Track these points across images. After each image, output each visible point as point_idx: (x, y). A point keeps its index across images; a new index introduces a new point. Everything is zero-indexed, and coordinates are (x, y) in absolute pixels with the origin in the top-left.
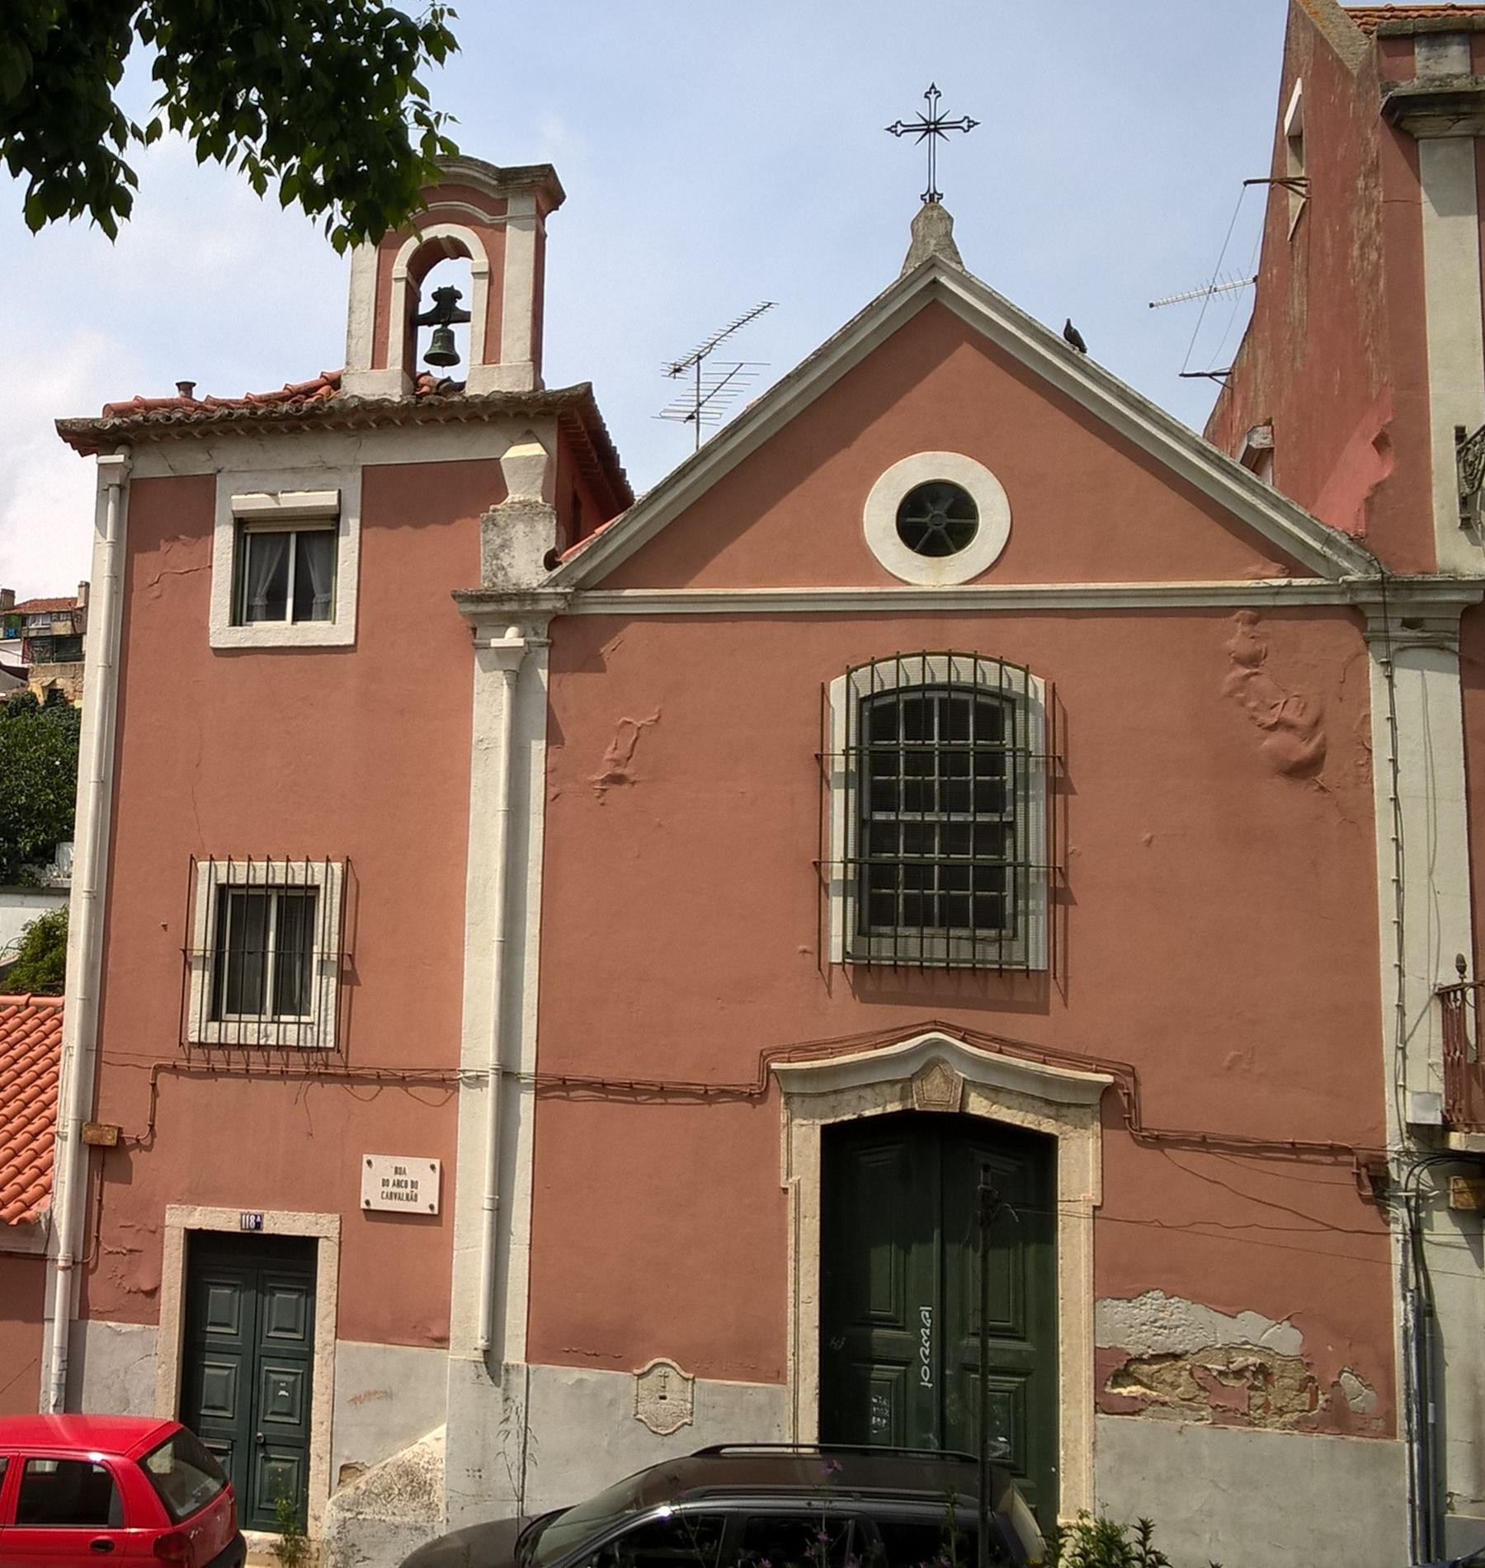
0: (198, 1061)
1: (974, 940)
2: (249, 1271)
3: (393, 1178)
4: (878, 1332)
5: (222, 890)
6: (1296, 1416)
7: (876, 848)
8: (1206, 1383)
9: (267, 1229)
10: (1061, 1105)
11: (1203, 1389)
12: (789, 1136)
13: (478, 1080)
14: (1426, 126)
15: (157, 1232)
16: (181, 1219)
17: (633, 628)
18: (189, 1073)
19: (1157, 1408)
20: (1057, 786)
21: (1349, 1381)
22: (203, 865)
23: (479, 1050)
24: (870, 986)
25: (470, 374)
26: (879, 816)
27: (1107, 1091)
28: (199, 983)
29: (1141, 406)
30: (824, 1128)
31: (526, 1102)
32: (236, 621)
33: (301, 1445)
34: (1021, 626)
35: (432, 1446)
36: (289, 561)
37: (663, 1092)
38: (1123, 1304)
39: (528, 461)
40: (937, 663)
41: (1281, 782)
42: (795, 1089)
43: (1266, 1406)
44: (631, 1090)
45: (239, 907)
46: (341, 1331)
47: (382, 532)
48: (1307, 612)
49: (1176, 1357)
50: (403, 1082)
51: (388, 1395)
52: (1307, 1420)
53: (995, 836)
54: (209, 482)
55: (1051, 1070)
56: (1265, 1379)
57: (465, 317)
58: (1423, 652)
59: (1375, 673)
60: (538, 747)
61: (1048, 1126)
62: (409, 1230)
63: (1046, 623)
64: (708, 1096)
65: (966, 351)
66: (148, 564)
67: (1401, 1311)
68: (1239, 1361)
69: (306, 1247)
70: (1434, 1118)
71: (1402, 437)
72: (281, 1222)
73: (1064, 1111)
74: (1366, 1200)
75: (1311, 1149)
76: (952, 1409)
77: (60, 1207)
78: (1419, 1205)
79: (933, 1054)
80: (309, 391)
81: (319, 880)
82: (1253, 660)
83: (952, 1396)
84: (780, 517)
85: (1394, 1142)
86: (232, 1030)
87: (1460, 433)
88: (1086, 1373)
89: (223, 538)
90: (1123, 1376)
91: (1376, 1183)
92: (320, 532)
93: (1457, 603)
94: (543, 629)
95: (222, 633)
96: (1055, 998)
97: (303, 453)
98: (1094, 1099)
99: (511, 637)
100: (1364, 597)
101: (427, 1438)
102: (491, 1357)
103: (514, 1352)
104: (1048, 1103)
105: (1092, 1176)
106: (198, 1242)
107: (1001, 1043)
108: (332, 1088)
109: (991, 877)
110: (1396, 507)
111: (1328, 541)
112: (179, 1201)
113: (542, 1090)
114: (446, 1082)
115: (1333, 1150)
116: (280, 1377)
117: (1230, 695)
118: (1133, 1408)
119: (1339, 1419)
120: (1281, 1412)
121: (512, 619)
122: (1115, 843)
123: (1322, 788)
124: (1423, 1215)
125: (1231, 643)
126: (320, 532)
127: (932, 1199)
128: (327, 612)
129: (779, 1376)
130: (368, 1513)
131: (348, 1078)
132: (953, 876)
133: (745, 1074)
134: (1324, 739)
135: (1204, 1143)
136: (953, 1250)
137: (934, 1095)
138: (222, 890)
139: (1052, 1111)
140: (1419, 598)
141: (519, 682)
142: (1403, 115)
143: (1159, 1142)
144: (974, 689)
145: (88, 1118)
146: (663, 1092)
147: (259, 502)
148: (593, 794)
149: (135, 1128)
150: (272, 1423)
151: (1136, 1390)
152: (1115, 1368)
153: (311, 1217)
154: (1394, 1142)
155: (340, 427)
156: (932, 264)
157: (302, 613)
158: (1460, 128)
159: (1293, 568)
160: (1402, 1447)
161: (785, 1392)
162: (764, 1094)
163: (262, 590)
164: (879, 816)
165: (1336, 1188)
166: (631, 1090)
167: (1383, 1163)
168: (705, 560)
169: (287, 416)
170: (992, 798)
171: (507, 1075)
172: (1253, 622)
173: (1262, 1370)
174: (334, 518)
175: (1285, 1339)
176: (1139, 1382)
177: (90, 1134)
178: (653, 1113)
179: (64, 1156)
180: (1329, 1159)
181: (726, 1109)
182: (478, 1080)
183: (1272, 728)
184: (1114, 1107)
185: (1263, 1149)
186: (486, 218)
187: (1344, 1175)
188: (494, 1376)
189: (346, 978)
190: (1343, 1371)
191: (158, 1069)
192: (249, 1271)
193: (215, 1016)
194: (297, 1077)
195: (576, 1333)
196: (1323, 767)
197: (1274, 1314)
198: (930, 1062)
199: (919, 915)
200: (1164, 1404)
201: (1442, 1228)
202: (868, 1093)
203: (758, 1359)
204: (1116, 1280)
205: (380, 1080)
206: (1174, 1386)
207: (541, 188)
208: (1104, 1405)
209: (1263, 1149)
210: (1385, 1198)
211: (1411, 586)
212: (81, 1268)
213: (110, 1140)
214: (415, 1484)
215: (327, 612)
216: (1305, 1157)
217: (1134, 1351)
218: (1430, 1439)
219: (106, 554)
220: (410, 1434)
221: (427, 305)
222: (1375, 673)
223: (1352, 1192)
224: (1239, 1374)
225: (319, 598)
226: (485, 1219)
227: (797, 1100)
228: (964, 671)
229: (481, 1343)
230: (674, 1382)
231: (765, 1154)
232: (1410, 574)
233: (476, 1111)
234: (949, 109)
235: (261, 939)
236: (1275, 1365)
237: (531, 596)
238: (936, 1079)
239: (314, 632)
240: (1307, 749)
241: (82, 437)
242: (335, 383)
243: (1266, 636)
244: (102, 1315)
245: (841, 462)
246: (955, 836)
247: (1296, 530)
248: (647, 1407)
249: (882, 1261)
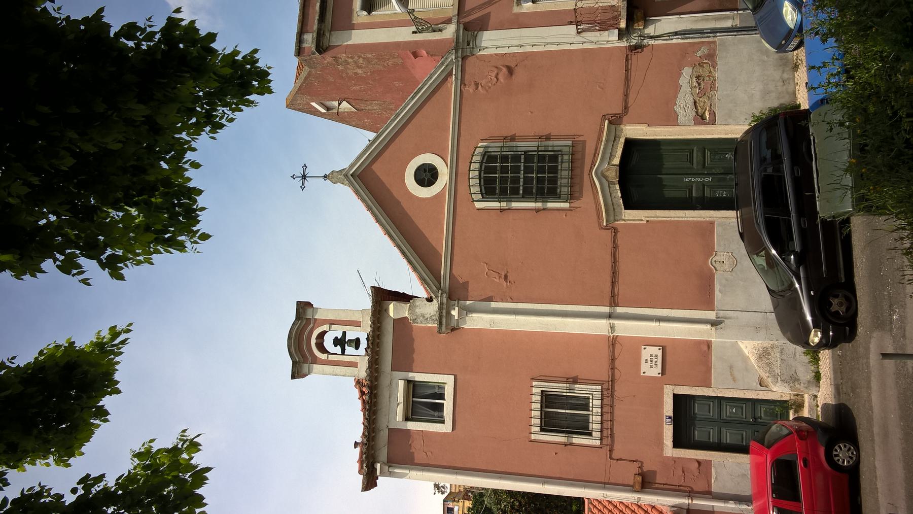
0: (607, 441)
1: (562, 162)
2: (688, 422)
3: (649, 364)
4: (694, 195)
5: (542, 430)
7: (532, 193)
8: (703, 93)
9: (671, 414)
13: (612, 327)
14: (325, 43)
15: (675, 460)
16: (669, 450)
17: (454, 272)
18: (612, 445)
20: (513, 138)
21: (699, 54)
22: (533, 437)
23: (600, 327)
24: (577, 195)
25: (362, 334)
26: (521, 192)
27: (610, 123)
28: (577, 440)
31: (619, 310)
32: (443, 422)
33: (754, 402)
34: (461, 150)
35: (748, 347)
36: (425, 403)
37: (614, 262)
39: (394, 308)
40: (472, 174)
41: (514, 77)
42: (612, 218)
43: (709, 76)
44: (614, 273)
45: (549, 424)
46: (708, 386)
47: (414, 364)
48: (463, 71)
49: (695, 102)
50: (613, 360)
51: (731, 367)
53: (528, 157)
54: (391, 431)
57: (344, 333)
59: (482, 53)
60: (494, 305)
61: (622, 140)
62: (668, 358)
63: (461, 143)
64: (615, 247)
65: (375, 167)
66: (419, 457)
67: (676, 40)
68: (695, 84)
69: (676, 397)
70: (616, 31)
71: (414, 50)
72: (668, 408)
74: (642, 51)
75: (627, 66)
76: (718, 171)
77: (665, 501)
78: (643, 37)
79: (599, 172)
80: (362, 393)
81: (539, 390)
82: (477, 85)
84: (421, 223)
85: (624, 44)
86: (595, 426)
87: (414, 32)
88: (703, 128)
89: (412, 426)
90: (702, 117)
92: (413, 387)
94: (453, 302)
95: (446, 428)
96: (581, 138)
97: (384, 393)
98: (613, 127)
99: (455, 313)
100: (460, 54)
101: (746, 351)
102: (714, 323)
103: (711, 315)
105: (638, 127)
106: (677, 444)
108: (617, 388)
109: (541, 158)
110: (435, 50)
111: (442, 64)
112: (662, 450)
113: (614, 301)
114: (613, 342)
115: (627, 60)
116: (729, 411)
118: (713, 114)
119: (711, 56)
120: (710, 72)
121: (448, 313)
125: (471, 91)
126: (413, 387)
128: (441, 386)
129: (712, 223)
130: (778, 371)
131: (613, 380)
132: (541, 170)
133: (608, 234)
135: (626, 95)
137: (613, 174)
138: (542, 430)
141: (470, 310)
142: (321, 48)
143: (626, 108)
144: (481, 163)
145: (631, 488)
146: (614, 262)
147: (400, 410)
148: (510, 287)
149: (634, 468)
150: (746, 414)
153: (665, 396)
154: (624, 44)
155: (377, 379)
156: (346, 176)
157: (442, 397)
158: (327, 35)
159: (450, 74)
160: (719, 38)
161: (717, 221)
162: (615, 228)
163: (432, 413)
164: (521, 192)
165: (638, 60)
166: (614, 273)
167: (630, 46)
169: (370, 407)
170: (516, 158)
171: (610, 316)
172: (465, 85)
173: (698, 77)
174: (408, 382)
175: (687, 72)
177: (638, 487)
178: (622, 266)
181: (619, 241)
182: (612, 327)
184: (616, 121)
185: (627, 79)
186: (311, 325)
187: (634, 57)
188: (721, 323)
189: (575, 381)
191: (611, 458)
192: (688, 422)
193: (590, 434)
194: (613, 401)
195: (702, 292)
196: (509, 66)
197: (679, 75)
198: (602, 176)
199: (554, 181)
201: (650, 30)
202: (613, 195)
203: (708, 229)
204: (671, 119)
205: (613, 369)
206: (705, 102)
207: (303, 307)
208: (713, 122)
209: (627, 79)
211: (457, 42)
212: (691, 493)
213: (639, 479)
214: (764, 354)
215: (441, 386)
218: (714, 31)
219: (414, 473)
220: (745, 359)
221: (338, 349)
223: (639, 55)
224: (699, 84)
225: (437, 390)
226: (664, 325)
229: (709, 326)
230: (717, 258)
231: (634, 227)
232: (454, 44)
234: (299, 172)
235: (562, 415)
237: (441, 304)
238: (608, 174)
239: (449, 392)
240: (505, 70)
241: (370, 483)
242: (359, 383)
244: (710, 485)
245: (404, 204)
246: (528, 170)
248: (727, 268)
249: (669, 193)
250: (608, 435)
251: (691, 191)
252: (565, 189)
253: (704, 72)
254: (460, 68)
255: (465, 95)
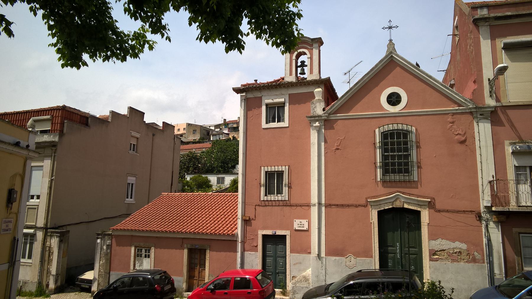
0: (263, 204)
1: (404, 176)
2: (274, 242)
3: (300, 223)
4: (389, 248)
5: (266, 172)
7: (385, 160)
8: (450, 255)
9: (277, 234)
13: (314, 205)
14: (480, 24)
15: (257, 235)
16: (261, 233)
18: (261, 206)
20: (418, 147)
21: (476, 253)
22: (262, 168)
23: (314, 199)
24: (385, 185)
25: (308, 76)
26: (386, 154)
27: (429, 202)
28: (263, 189)
29: (430, 77)
31: (323, 209)
32: (267, 123)
33: (285, 273)
34: (410, 118)
35: (309, 272)
36: (275, 112)
37: (348, 206)
39: (319, 91)
40: (395, 125)
41: (459, 145)
42: (372, 204)
44: (342, 206)
45: (269, 175)
46: (291, 252)
47: (293, 105)
48: (462, 113)
49: (444, 250)
50: (301, 206)
51: (300, 263)
53: (407, 157)
54: (261, 98)
55: (419, 199)
57: (306, 66)
59: (475, 124)
60: (323, 144)
61: (419, 209)
62: (303, 233)
63: (415, 117)
64: (356, 206)
65: (398, 68)
66: (250, 113)
67: (485, 240)
68: (456, 251)
69: (284, 237)
70: (489, 205)
71: (478, 81)
72: (279, 232)
74: (477, 220)
75: (467, 211)
76: (404, 261)
77: (239, 231)
78: (487, 221)
80: (278, 80)
81: (284, 170)
82: (453, 123)
83: (403, 259)
84: (365, 100)
85: (482, 210)
86: (269, 198)
87: (489, 79)
88: (428, 254)
89: (264, 108)
90: (434, 254)
91: (479, 217)
92: (281, 106)
94: (323, 122)
95: (264, 125)
96: (419, 186)
97: (278, 92)
98: (427, 204)
99: (317, 124)
100: (473, 110)
101: (308, 271)
102: (319, 255)
103: (323, 254)
105: (427, 218)
106: (264, 236)
107: (410, 194)
108: (288, 208)
109: (407, 164)
110: (478, 93)
111: (466, 100)
113: (326, 206)
114: (309, 206)
115: (471, 211)
116: (280, 261)
118: (437, 260)
119: (474, 260)
120: (464, 259)
121: (317, 121)
125: (449, 120)
126: (281, 106)
127: (398, 223)
128: (283, 121)
129: (372, 257)
130: (298, 285)
131: (291, 206)
132: (400, 164)
133: (363, 202)
135: (448, 211)
136: (402, 232)
137: (398, 204)
138: (266, 172)
141: (319, 132)
142: (476, 22)
143: (439, 211)
144: (402, 130)
145: (243, 215)
146: (348, 206)
147: (270, 101)
148: (333, 152)
149: (252, 216)
150: (279, 269)
151: (437, 257)
152: (433, 253)
153: (285, 231)
154: (482, 210)
155: (284, 87)
156: (391, 53)
157: (279, 121)
158: (487, 24)
159: (460, 105)
160: (486, 265)
161: (373, 260)
162: (367, 205)
163: (271, 117)
164: (386, 154)
165: (472, 218)
166: (342, 206)
168: (352, 108)
169: (274, 85)
170: (406, 150)
171: (320, 204)
172: (453, 116)
173: (460, 252)
174: (284, 103)
175: (464, 246)
177: (244, 218)
178: (347, 210)
179: (239, 222)
181: (360, 209)
182: (314, 205)
183: (457, 135)
184: (431, 205)
185: (458, 212)
186: (309, 47)
188: (320, 259)
189: (290, 187)
191: (256, 205)
192: (274, 242)
193: (266, 195)
194: (281, 206)
195: (334, 250)
196: (466, 141)
197: (462, 242)
198: (397, 198)
199: (394, 172)
201: (492, 225)
203: (368, 254)
204: (432, 237)
205: (296, 206)
206: (444, 256)
207: (319, 42)
208: (431, 260)
209: (458, 212)
211: (481, 108)
212: (243, 242)
213: (248, 219)
214: (306, 279)
215: (283, 121)
218: (491, 264)
219: (243, 112)
220: (305, 270)
221: (299, 64)
222: (475, 124)
223: (475, 219)
224: (456, 253)
225: (282, 118)
226: (317, 230)
228: (400, 127)
229: (317, 253)
230: (353, 259)
232: (481, 106)
233: (314, 211)
234: (393, 24)
235: (274, 181)
236: (462, 251)
237: (320, 116)
239: (281, 124)
240: (463, 138)
241: (237, 90)
242: (283, 79)
244: (248, 251)
246: (400, 157)
248: (348, 263)
249: (390, 235)
250: (266, 204)
251: (392, 246)
252: (388, 178)
253: (464, 255)
254: (463, 111)
255: (446, 116)
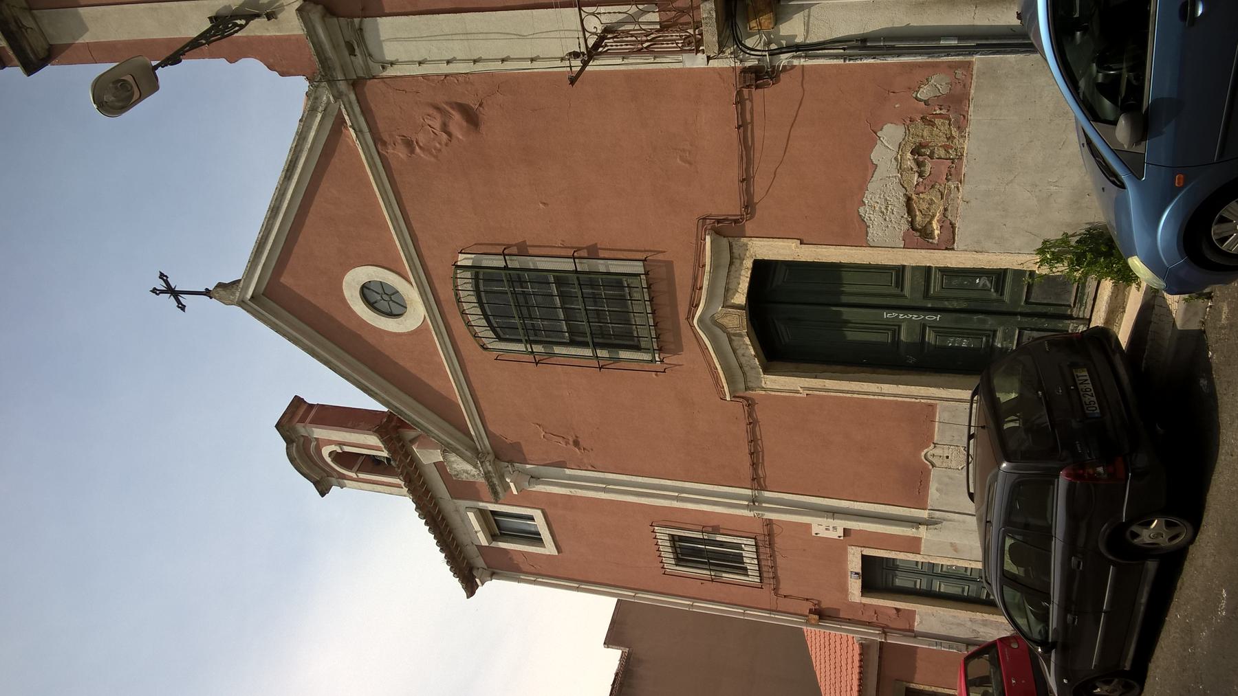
6: (954, 130)
10: (732, 258)
11: (933, 187)
12: (772, 390)
17: (491, 428)
19: (949, 214)
21: (925, 93)
29: (274, 210)
30: (766, 371)
37: (753, 440)
38: (870, 230)
41: (483, 128)
43: (946, 148)
49: (909, 200)
52: (957, 121)
56: (924, 147)
58: (368, 42)
59: (390, 72)
60: (568, 471)
61: (748, 264)
73: (736, 255)
79: (708, 321)
82: (409, 144)
91: (759, 76)
93: (327, 29)
96: (660, 257)
104: (731, 263)
107: (696, 288)
117: (436, 157)
118: (950, 229)
122: (550, 228)
123: (480, 105)
124: (784, 42)
134: (447, 103)
135: (746, 180)
137: (737, 322)
139: (737, 262)
140: (330, 53)
143: (749, 206)
151: (935, 225)
152: (920, 235)
159: (340, 122)
167: (745, 71)
172: (384, 143)
175: (891, 135)
176: (930, 223)
180: (748, 104)
183: (449, 134)
184: (727, 229)
185: (746, 146)
187: (757, 94)
190: (916, 98)
196: (466, 104)
197: (873, 139)
198: (711, 324)
200: (946, 210)
201: (793, 29)
202: (740, 352)
203: (927, 412)
206: (931, 202)
210: (773, 72)
216: (748, 117)
217: (905, 226)
222: (390, 72)
224: (920, 164)
227: (750, 384)
231: (787, 402)
236: (912, 142)
238: (725, 321)
243: (391, 136)
247: (315, 127)
252: (643, 332)
253: (935, 136)
254: (357, 109)
255: (394, 164)
